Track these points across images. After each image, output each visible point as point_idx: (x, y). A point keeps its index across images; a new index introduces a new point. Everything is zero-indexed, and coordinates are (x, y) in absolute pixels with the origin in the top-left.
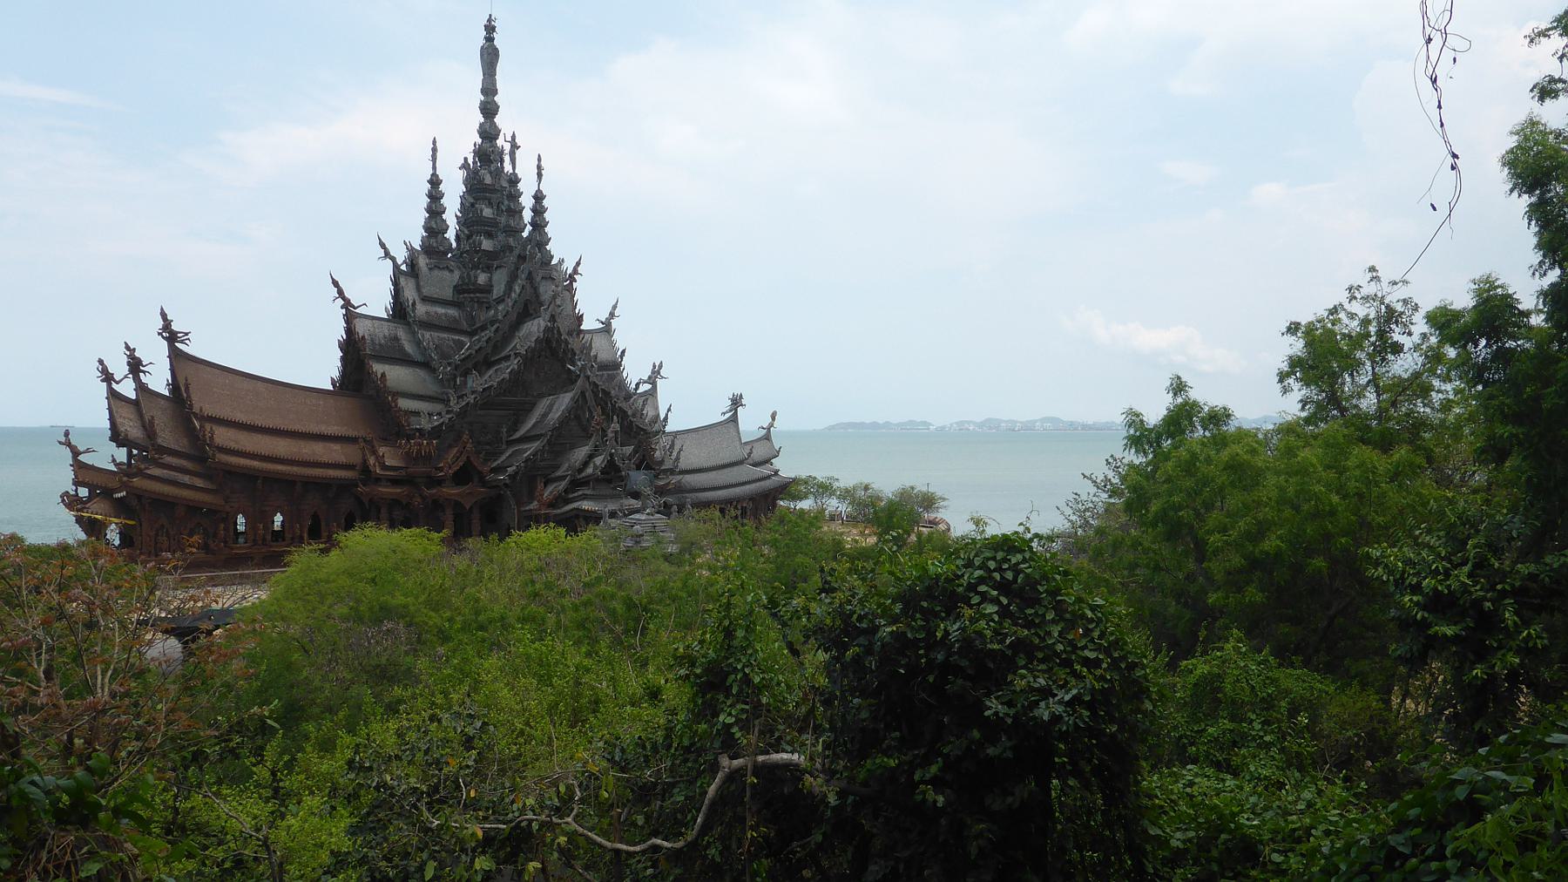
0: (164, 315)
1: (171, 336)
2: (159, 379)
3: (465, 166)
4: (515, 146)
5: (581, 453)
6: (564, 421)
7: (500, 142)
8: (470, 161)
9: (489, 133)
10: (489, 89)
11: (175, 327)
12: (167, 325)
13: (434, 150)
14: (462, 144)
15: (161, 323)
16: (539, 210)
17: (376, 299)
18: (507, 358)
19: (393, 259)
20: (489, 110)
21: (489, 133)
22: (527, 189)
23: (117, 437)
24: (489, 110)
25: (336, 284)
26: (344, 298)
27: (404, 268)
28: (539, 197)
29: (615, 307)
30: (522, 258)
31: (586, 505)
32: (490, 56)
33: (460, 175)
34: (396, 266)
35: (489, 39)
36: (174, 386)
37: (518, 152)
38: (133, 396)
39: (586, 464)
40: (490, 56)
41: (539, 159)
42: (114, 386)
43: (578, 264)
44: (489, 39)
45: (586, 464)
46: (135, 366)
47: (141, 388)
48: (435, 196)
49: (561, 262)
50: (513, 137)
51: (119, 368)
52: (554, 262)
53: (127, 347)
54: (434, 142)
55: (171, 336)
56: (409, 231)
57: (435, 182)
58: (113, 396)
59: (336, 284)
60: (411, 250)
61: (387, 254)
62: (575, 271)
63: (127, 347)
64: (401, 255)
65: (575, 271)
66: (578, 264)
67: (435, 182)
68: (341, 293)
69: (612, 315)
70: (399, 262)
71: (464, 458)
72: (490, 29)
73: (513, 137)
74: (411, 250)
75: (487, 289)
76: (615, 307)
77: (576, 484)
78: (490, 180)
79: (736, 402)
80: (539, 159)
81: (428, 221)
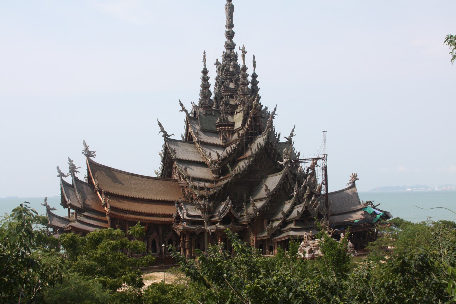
0: (85, 144)
1: (88, 154)
2: (82, 175)
3: (217, 63)
4: (244, 52)
5: (287, 207)
6: (277, 190)
7: (236, 50)
8: (221, 61)
9: (230, 46)
10: (230, 25)
11: (90, 149)
12: (87, 149)
14: (217, 53)
15: (83, 148)
16: (255, 82)
17: (178, 131)
18: (246, 158)
19: (186, 111)
20: (230, 35)
21: (230, 46)
22: (250, 72)
23: (64, 203)
24: (230, 35)
25: (160, 125)
27: (191, 115)
29: (293, 130)
30: (250, 108)
31: (292, 233)
33: (215, 68)
34: (188, 115)
36: (89, 178)
37: (246, 55)
38: (71, 183)
39: (290, 211)
41: (254, 57)
42: (63, 178)
43: (275, 109)
45: (290, 211)
46: (73, 169)
47: (76, 179)
48: (205, 79)
49: (266, 108)
50: (244, 47)
51: (66, 171)
52: (263, 108)
53: (70, 160)
54: (205, 53)
55: (88, 154)
56: (193, 97)
57: (205, 72)
58: (64, 184)
59: (160, 125)
60: (195, 107)
61: (184, 109)
62: (274, 113)
63: (70, 160)
64: (190, 109)
65: (274, 113)
66: (275, 109)
67: (205, 72)
69: (292, 135)
70: (189, 112)
71: (228, 211)
73: (244, 47)
74: (195, 107)
75: (233, 124)
76: (293, 130)
77: (285, 223)
79: (355, 178)
80: (254, 57)
81: (202, 91)
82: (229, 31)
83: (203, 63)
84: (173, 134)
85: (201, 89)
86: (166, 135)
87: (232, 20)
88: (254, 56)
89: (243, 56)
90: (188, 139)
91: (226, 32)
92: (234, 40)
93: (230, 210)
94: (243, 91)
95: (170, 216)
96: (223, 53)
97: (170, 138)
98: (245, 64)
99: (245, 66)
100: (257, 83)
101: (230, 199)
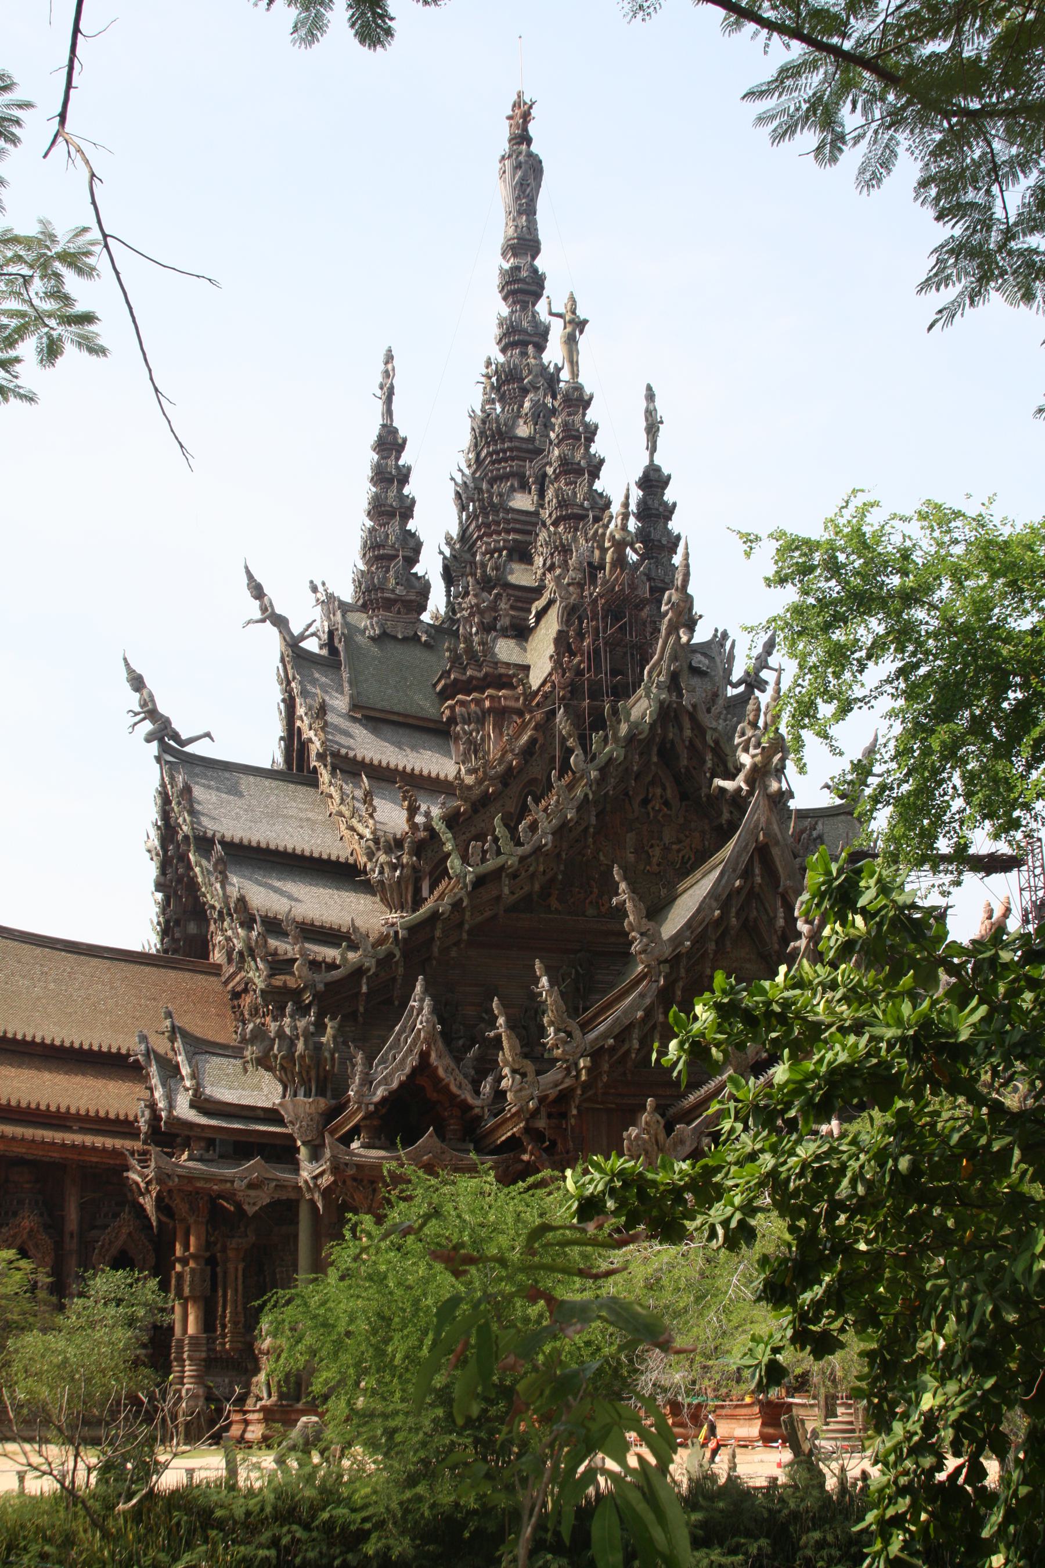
10: (525, 244)
19: (280, 622)
21: (522, 336)
24: (523, 287)
25: (137, 682)
27: (312, 645)
28: (653, 482)
32: (526, 173)
35: (521, 137)
40: (526, 173)
41: (650, 396)
44: (521, 137)
54: (389, 358)
56: (324, 561)
57: (390, 443)
60: (330, 603)
64: (305, 615)
67: (390, 443)
68: (151, 713)
71: (412, 1061)
72: (522, 117)
78: (531, 425)
80: (650, 396)
82: (516, 269)
83: (379, 406)
84: (208, 735)
85: (369, 524)
86: (164, 734)
87: (532, 226)
88: (649, 388)
89: (571, 341)
90: (297, 767)
91: (503, 273)
93: (424, 1056)
94: (562, 504)
95: (124, 1127)
96: (489, 364)
97: (189, 749)
98: (580, 380)
99: (579, 388)
100: (669, 511)
101: (426, 991)
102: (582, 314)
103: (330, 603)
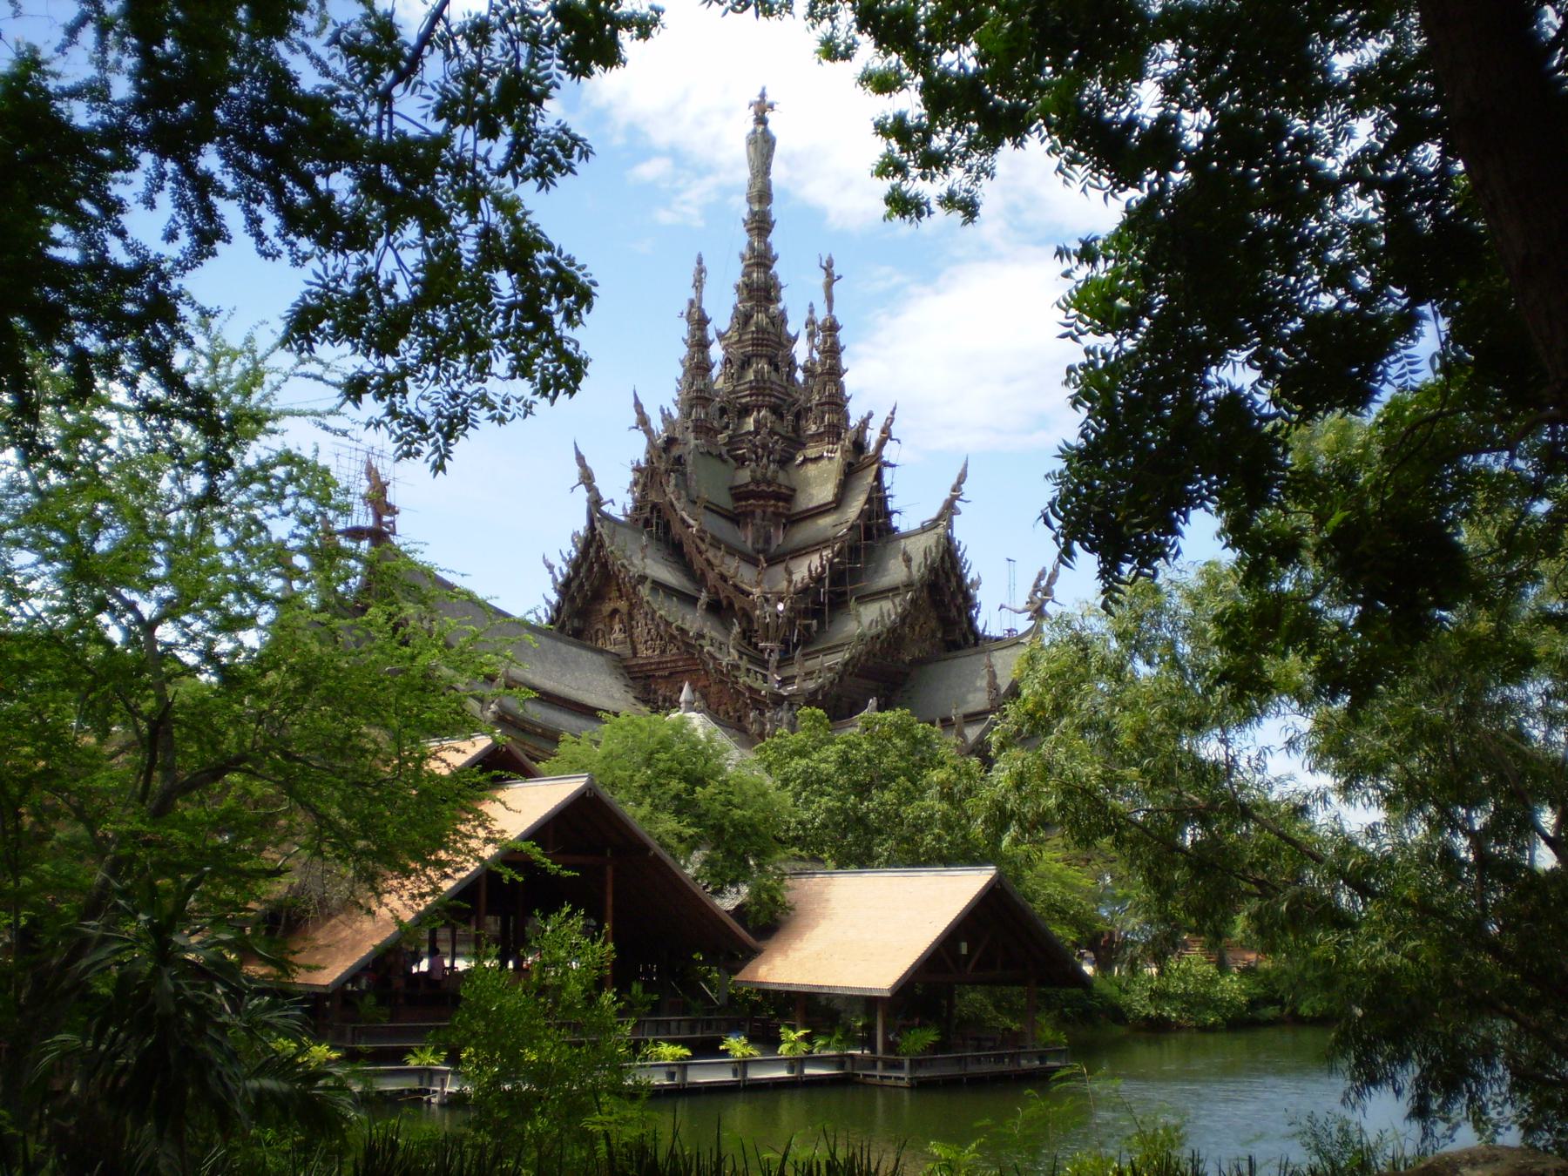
9: (761, 259)
11: (391, 497)
13: (701, 271)
19: (649, 432)
25: (580, 459)
26: (591, 488)
37: (836, 287)
54: (700, 262)
57: (699, 321)
59: (580, 459)
61: (643, 422)
92: (772, 238)
102: (836, 271)
103: (667, 418)
